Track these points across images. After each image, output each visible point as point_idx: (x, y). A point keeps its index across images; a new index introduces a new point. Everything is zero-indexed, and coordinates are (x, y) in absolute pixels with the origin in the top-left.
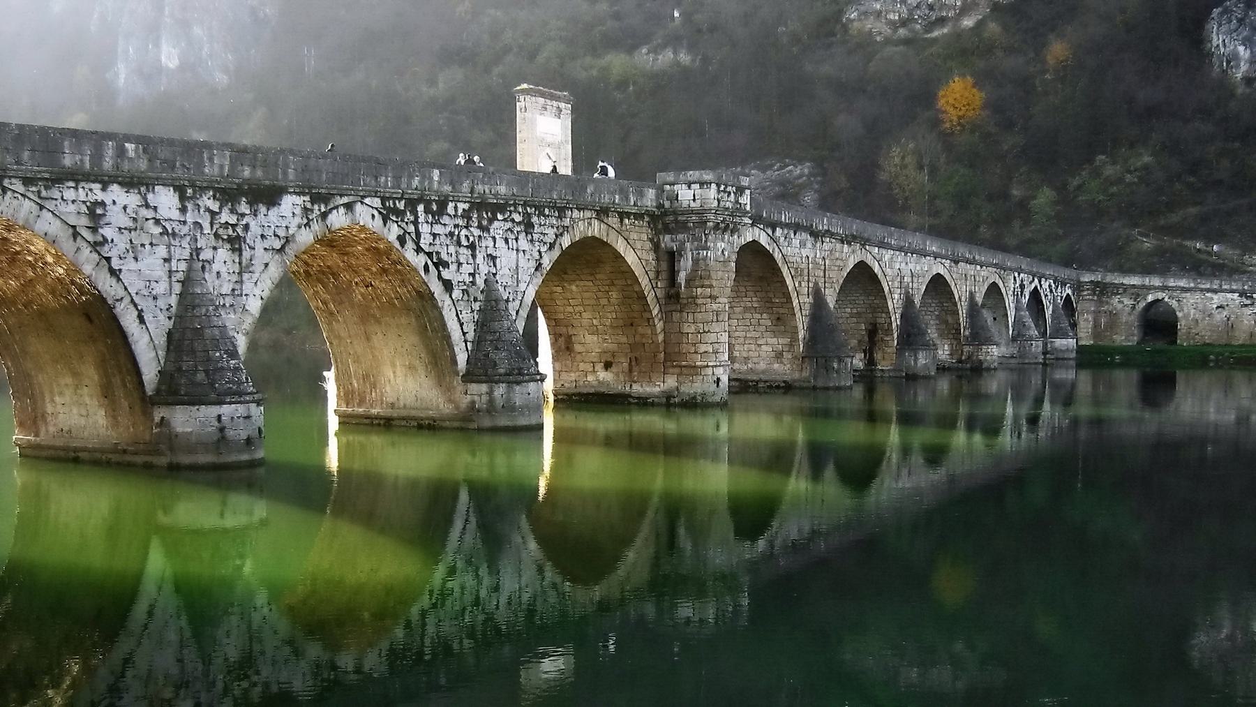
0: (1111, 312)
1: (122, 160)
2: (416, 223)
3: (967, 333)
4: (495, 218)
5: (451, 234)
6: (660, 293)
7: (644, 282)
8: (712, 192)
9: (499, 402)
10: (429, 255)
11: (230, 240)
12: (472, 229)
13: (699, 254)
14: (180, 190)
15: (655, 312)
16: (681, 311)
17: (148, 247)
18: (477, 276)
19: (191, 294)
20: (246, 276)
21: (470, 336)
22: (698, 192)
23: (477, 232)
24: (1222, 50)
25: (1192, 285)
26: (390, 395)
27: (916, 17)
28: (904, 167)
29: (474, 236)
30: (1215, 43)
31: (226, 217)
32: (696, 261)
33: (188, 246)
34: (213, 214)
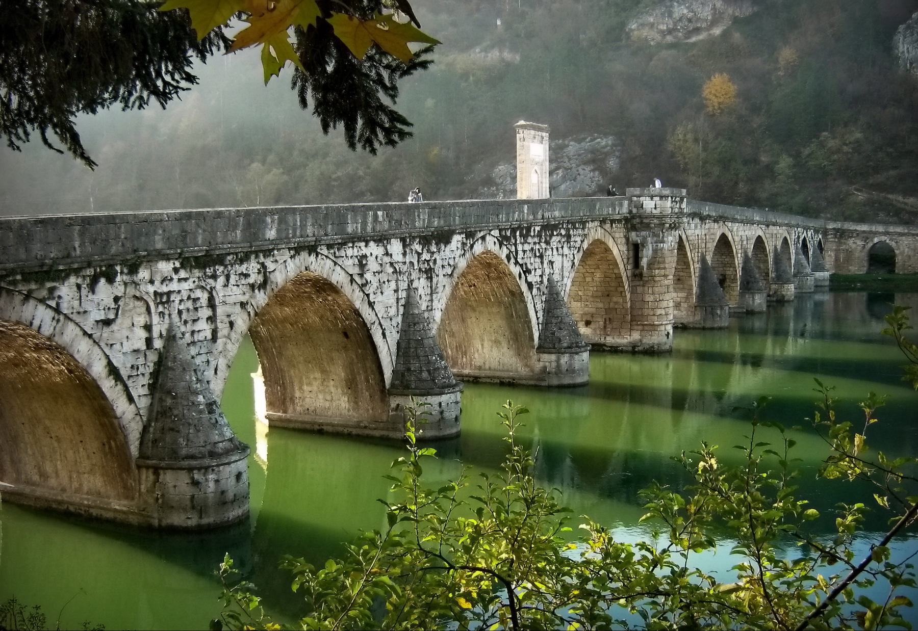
0: (847, 250)
1: (376, 224)
2: (515, 245)
3: (773, 276)
4: (552, 235)
5: (532, 249)
6: (629, 273)
7: (621, 266)
8: (668, 203)
9: (564, 367)
10: (521, 266)
11: (426, 272)
12: (541, 244)
13: (657, 246)
14: (403, 240)
15: (626, 287)
16: (643, 286)
17: (386, 283)
18: (544, 276)
19: (412, 314)
20: (434, 296)
21: (540, 320)
22: (659, 202)
23: (544, 245)
24: (907, 55)
25: (906, 231)
26: (478, 360)
27: (679, 27)
28: (685, 141)
29: (542, 249)
30: (901, 49)
31: (426, 256)
32: (655, 251)
33: (406, 280)
34: (419, 254)
